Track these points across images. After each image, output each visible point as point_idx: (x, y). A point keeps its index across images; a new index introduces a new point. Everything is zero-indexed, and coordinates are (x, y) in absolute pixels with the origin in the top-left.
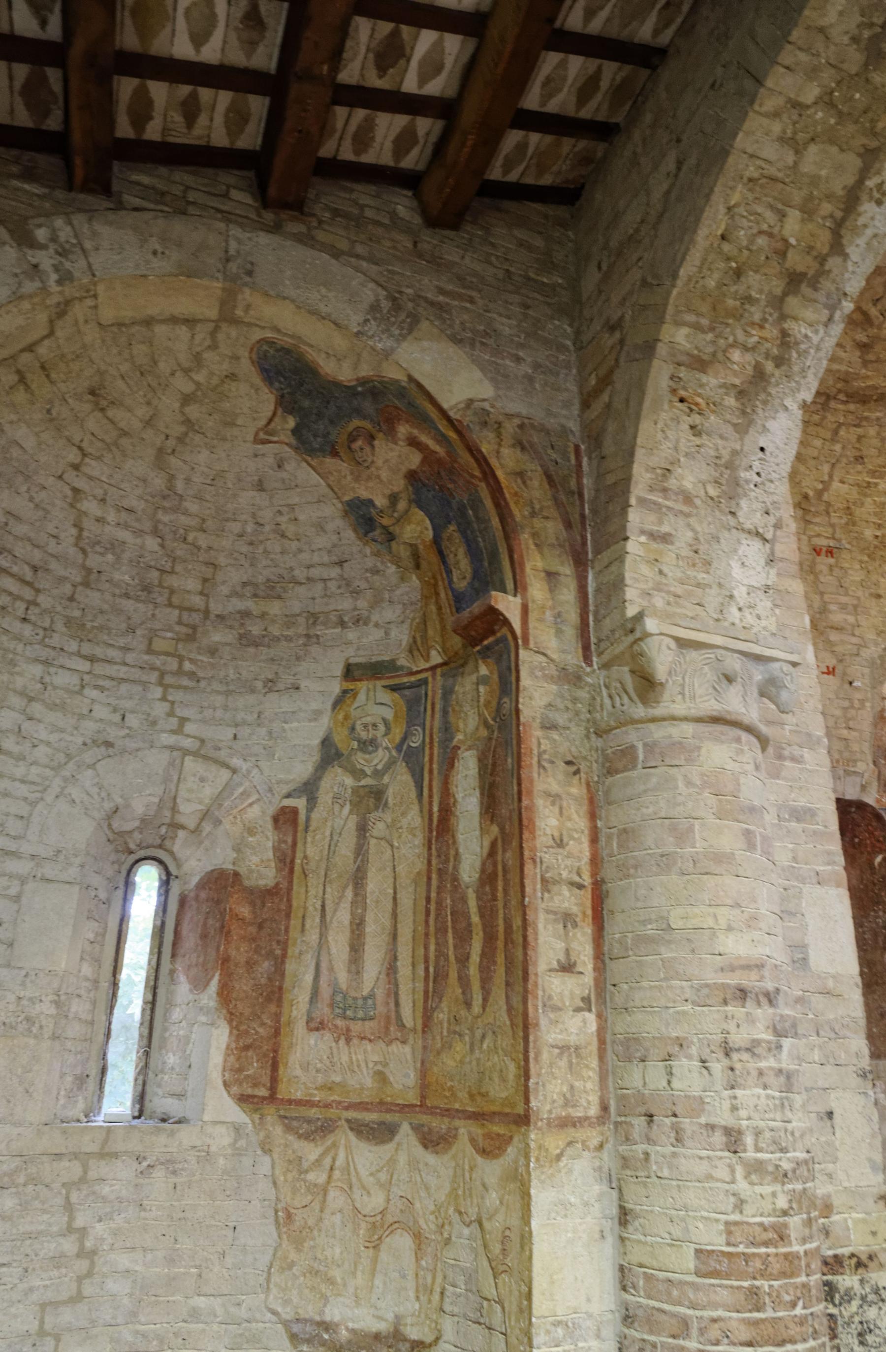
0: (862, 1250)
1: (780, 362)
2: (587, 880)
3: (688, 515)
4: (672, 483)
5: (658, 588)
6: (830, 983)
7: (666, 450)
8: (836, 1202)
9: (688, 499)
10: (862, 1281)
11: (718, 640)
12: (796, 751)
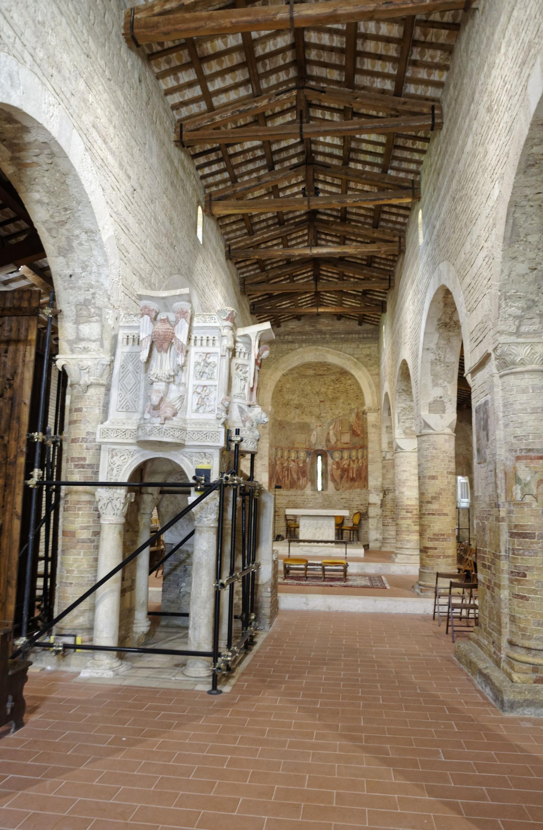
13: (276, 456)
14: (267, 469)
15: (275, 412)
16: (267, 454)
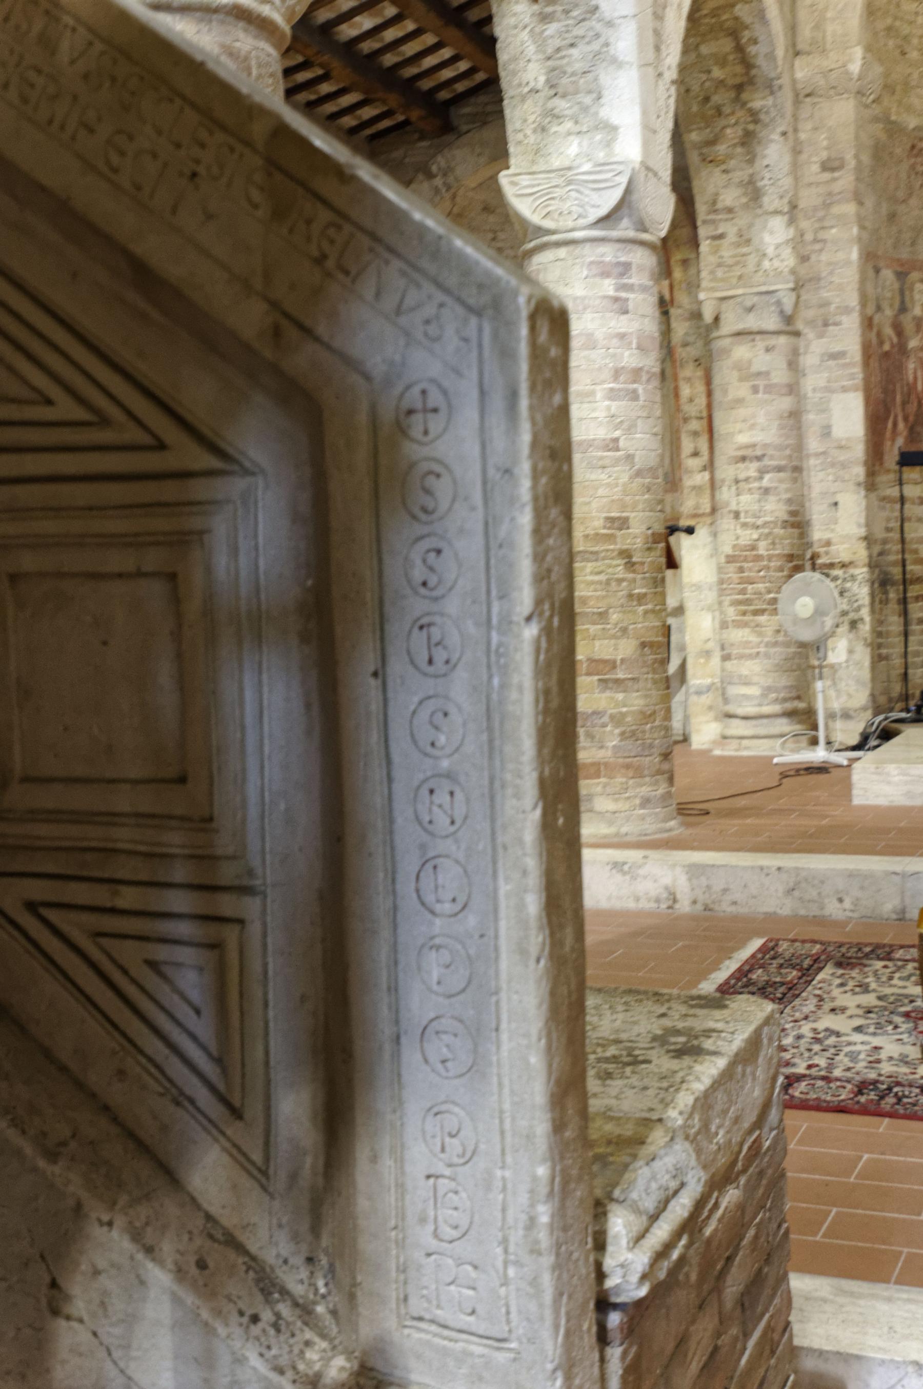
0: (845, 557)
1: (756, 121)
2: (705, 414)
3: (732, 219)
4: (720, 205)
5: (720, 265)
6: (843, 443)
7: (711, 189)
8: (834, 541)
9: (730, 210)
10: (845, 573)
11: (740, 291)
12: (838, 318)
13: (903, 309)
14: (857, 371)
15: (889, 88)
16: (853, 300)
